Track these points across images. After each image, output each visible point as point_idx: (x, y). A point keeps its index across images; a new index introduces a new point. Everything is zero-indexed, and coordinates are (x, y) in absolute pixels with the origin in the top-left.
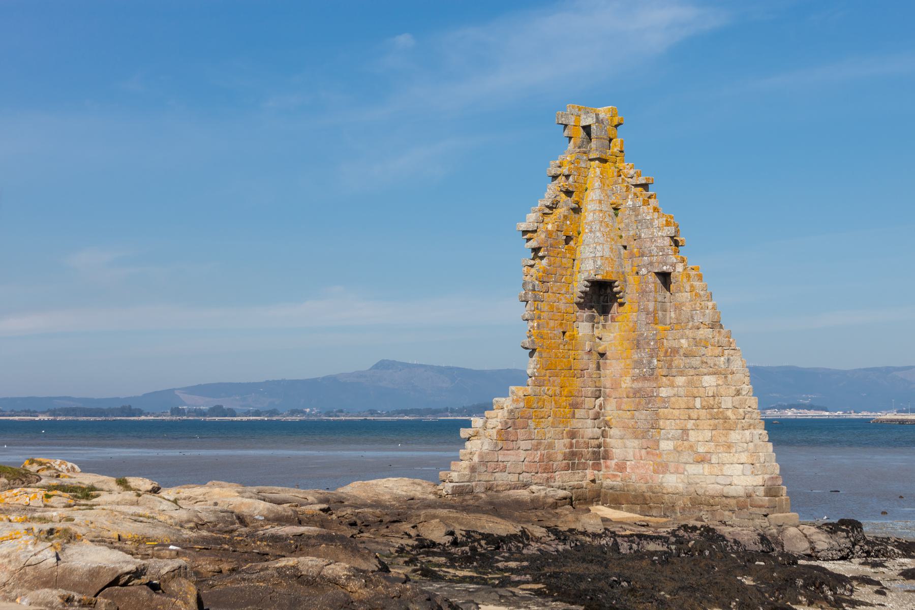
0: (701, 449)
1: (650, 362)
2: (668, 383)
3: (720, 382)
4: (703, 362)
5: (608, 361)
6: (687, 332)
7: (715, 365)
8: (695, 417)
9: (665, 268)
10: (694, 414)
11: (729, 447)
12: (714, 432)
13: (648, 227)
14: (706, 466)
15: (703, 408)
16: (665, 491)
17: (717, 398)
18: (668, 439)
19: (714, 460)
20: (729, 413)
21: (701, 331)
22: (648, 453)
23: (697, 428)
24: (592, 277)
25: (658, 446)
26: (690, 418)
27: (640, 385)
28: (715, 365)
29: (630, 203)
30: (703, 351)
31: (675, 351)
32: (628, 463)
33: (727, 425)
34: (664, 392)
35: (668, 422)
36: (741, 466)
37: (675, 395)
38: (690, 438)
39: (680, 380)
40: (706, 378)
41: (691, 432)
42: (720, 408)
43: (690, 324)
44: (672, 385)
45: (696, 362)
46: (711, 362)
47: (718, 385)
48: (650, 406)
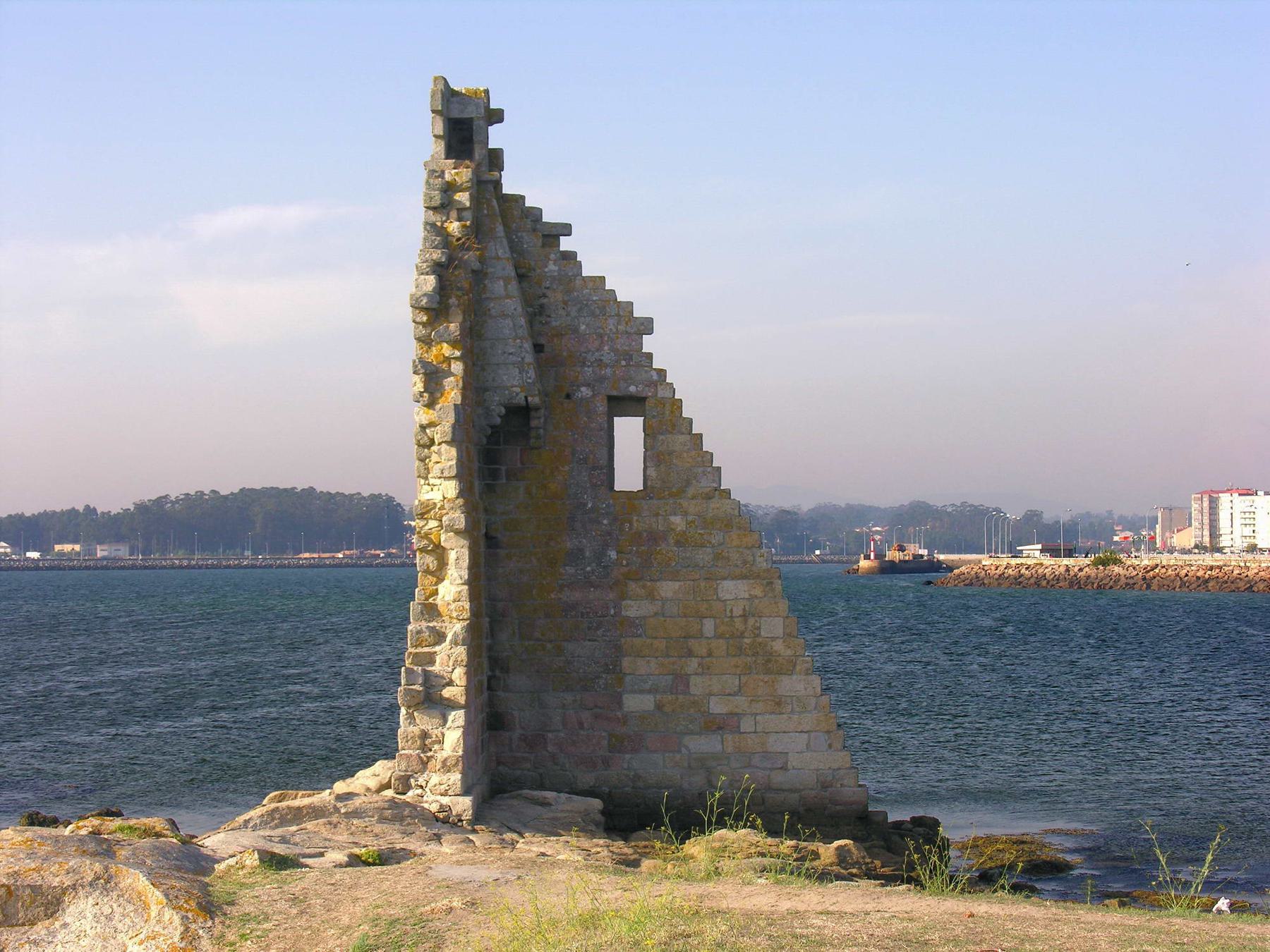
0: (717, 707)
1: (600, 556)
2: (642, 592)
3: (758, 592)
4: (718, 557)
5: (502, 552)
6: (685, 504)
7: (745, 562)
8: (704, 651)
9: (632, 389)
10: (700, 648)
11: (779, 704)
12: (744, 679)
13: (593, 314)
14: (729, 737)
15: (718, 636)
16: (640, 784)
17: (751, 621)
18: (642, 692)
19: (747, 725)
20: (778, 646)
21: (714, 504)
22: (596, 717)
23: (705, 670)
24: (520, 400)
25: (620, 704)
26: (690, 654)
27: (577, 595)
28: (745, 562)
29: (552, 267)
30: (716, 538)
31: (655, 538)
32: (550, 735)
33: (772, 666)
34: (633, 609)
35: (640, 662)
36: (806, 736)
37: (656, 614)
38: (693, 690)
39: (668, 588)
40: (728, 584)
41: (694, 680)
42: (759, 635)
43: (691, 491)
44: (651, 596)
45: (704, 556)
46: (735, 556)
47: (752, 598)
48: (599, 632)
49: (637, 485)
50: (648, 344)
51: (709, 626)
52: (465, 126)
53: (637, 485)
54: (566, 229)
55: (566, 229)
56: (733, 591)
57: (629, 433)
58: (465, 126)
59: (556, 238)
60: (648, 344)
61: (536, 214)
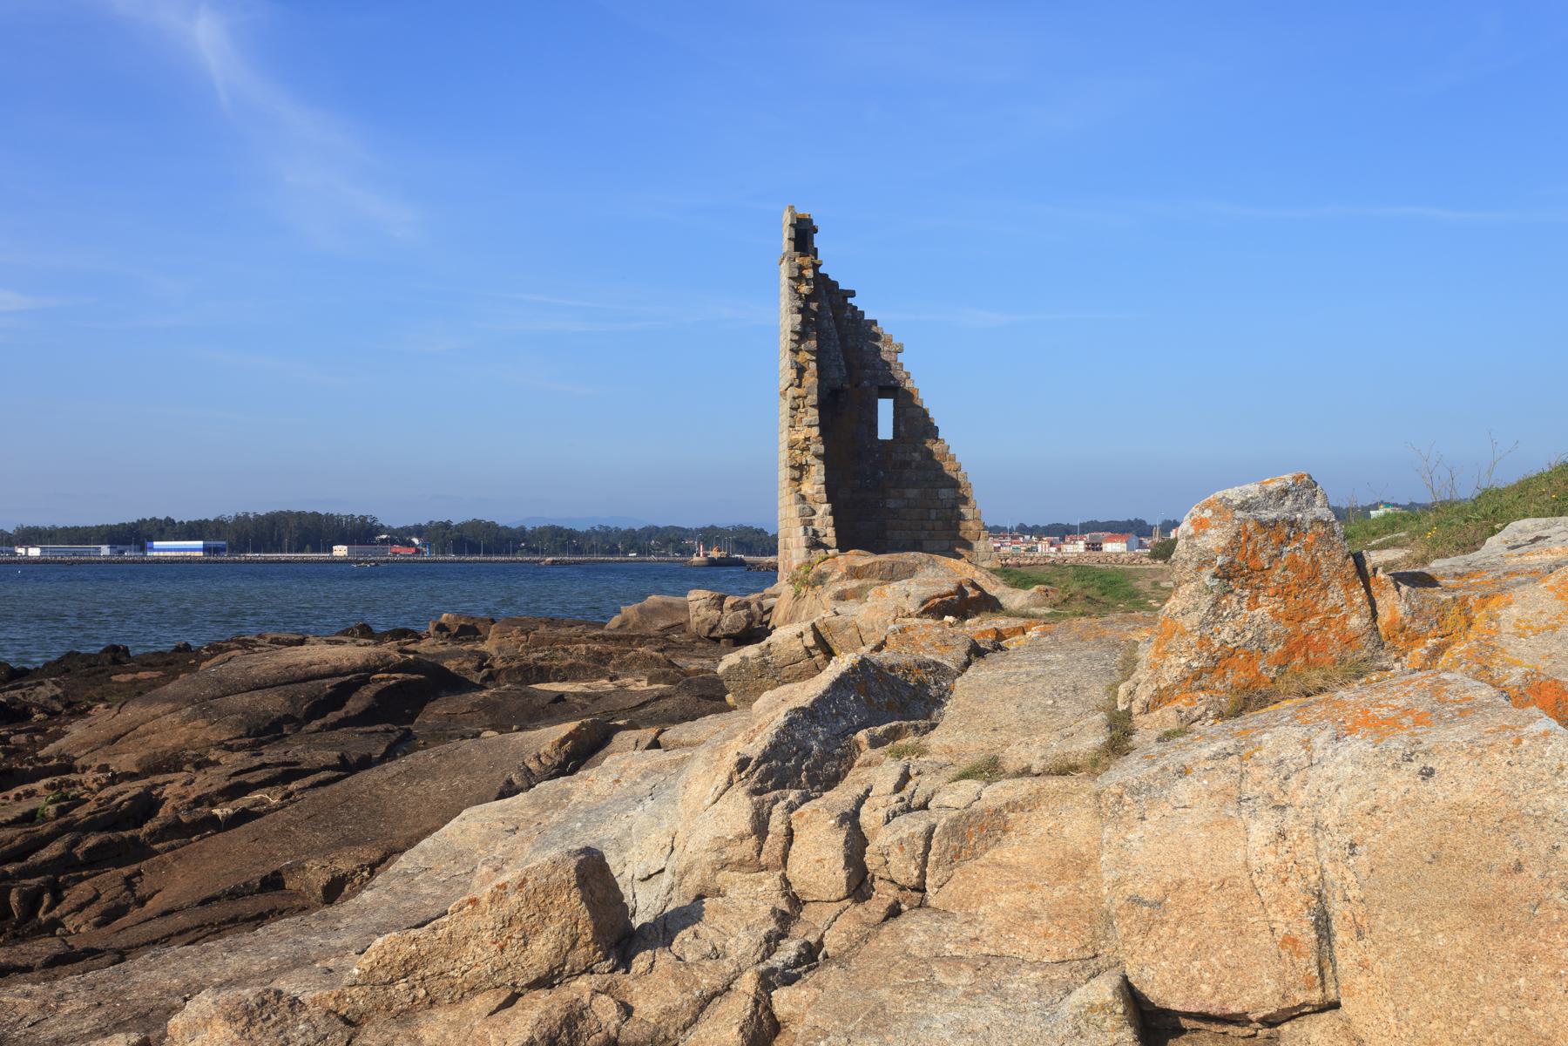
26: (923, 529)
31: (906, 464)
34: (891, 504)
39: (912, 493)
49: (890, 437)
50: (901, 358)
51: (933, 514)
52: (803, 234)
53: (890, 437)
54: (852, 294)
55: (852, 294)
56: (945, 493)
57: (885, 408)
58: (803, 234)
59: (845, 298)
60: (901, 358)
61: (835, 284)
